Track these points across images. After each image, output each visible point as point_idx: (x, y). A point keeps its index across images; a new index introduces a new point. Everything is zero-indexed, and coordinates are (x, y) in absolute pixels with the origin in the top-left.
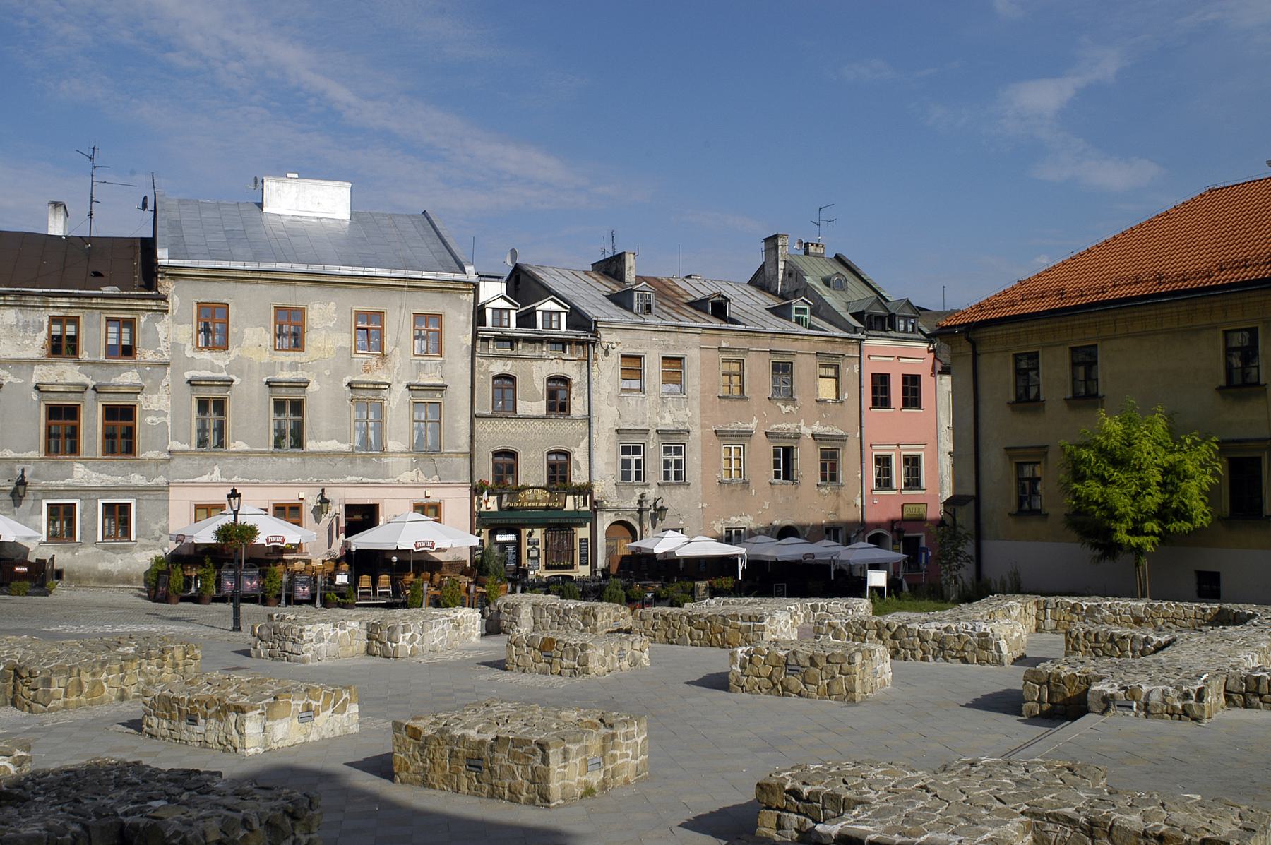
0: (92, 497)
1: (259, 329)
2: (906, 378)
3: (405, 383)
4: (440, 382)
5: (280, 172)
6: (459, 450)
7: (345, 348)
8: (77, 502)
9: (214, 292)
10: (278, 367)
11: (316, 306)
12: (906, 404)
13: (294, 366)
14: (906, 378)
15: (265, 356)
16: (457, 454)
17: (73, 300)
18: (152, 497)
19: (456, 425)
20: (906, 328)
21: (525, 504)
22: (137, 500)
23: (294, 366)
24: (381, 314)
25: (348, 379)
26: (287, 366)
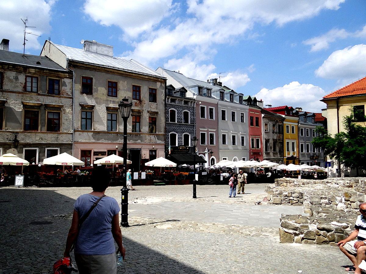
0: (43, 147)
1: (103, 88)
2: (256, 118)
3: (147, 110)
4: (156, 111)
8: (37, 149)
9: (88, 74)
14: (256, 118)
15: (105, 97)
17: (37, 70)
18: (66, 147)
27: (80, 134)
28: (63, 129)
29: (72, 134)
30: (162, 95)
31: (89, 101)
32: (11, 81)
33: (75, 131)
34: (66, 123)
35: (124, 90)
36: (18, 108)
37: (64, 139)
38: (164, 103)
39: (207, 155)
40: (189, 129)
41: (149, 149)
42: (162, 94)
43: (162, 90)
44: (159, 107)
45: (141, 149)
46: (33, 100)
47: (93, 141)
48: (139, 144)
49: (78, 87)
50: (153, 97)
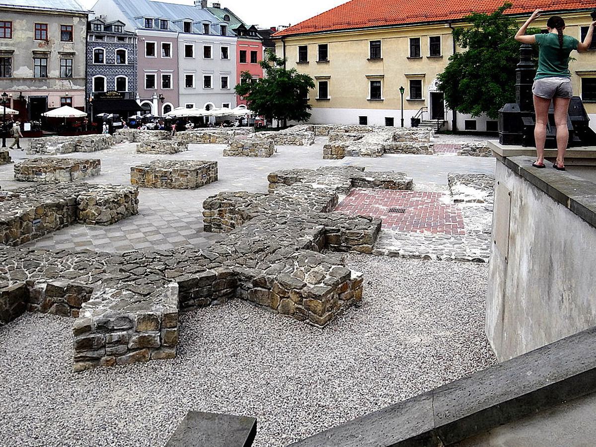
3: (57, 51)
4: (72, 51)
6: (81, 77)
7: (30, 38)
11: (17, 21)
12: (252, 61)
16: (79, 79)
20: (252, 33)
24: (46, 25)
30: (82, 32)
39: (155, 101)
41: (59, 96)
44: (78, 46)
48: (45, 91)
50: (67, 34)
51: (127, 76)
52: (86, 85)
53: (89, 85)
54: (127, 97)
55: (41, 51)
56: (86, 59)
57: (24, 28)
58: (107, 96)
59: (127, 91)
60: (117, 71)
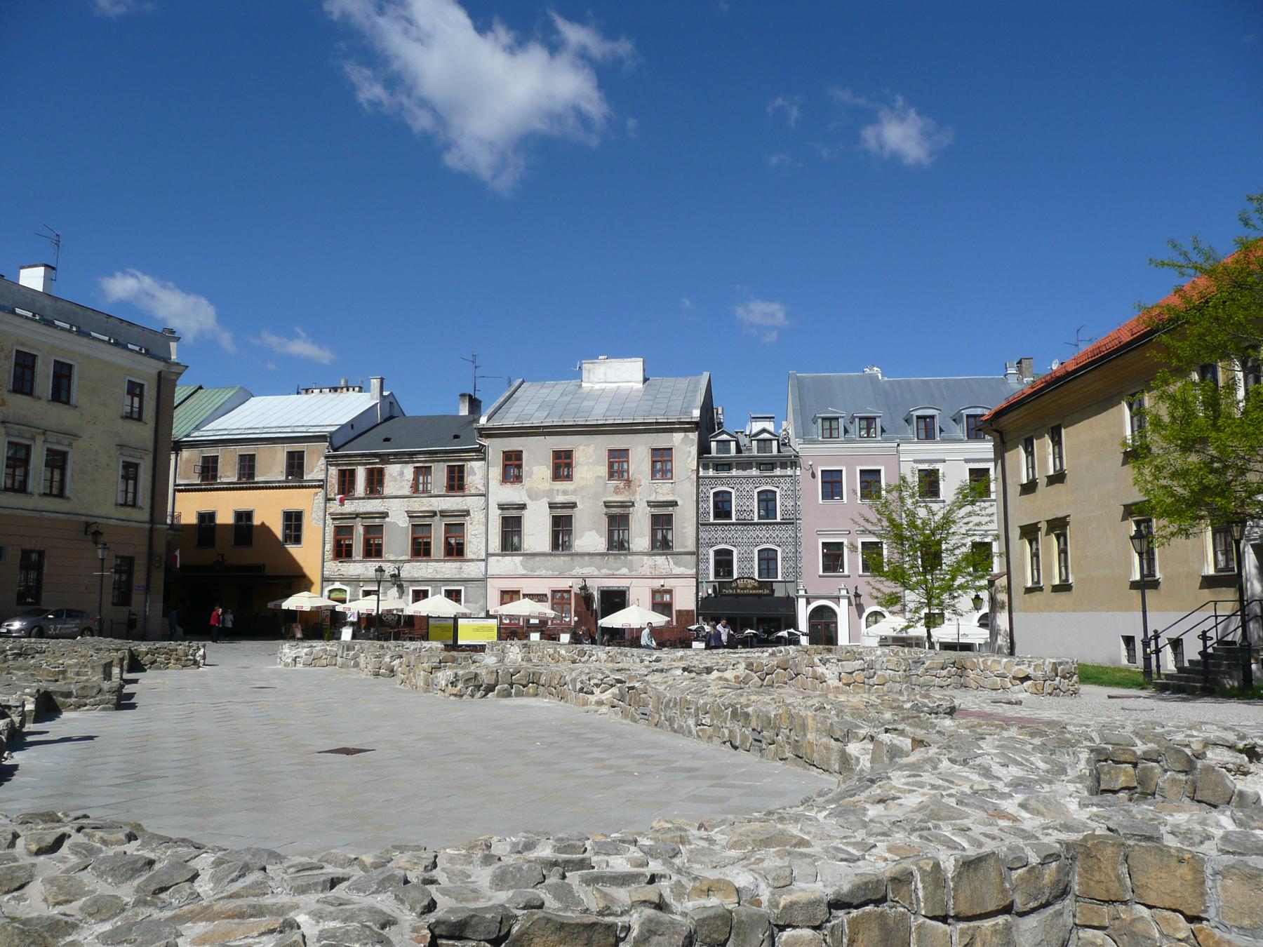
5: (593, 356)
7: (601, 477)
9: (513, 444)
10: (555, 493)
13: (565, 492)
19: (685, 531)
21: (738, 591)
22: (466, 587)
23: (565, 492)
25: (605, 499)
26: (563, 492)
27: (498, 561)
28: (469, 552)
29: (484, 560)
31: (511, 494)
32: (395, 479)
33: (488, 555)
34: (474, 540)
35: (588, 464)
36: (404, 522)
37: (471, 570)
38: (694, 477)
40: (777, 536)
42: (689, 456)
43: (688, 449)
45: (629, 588)
46: (423, 504)
47: (524, 572)
49: (496, 472)
51: (779, 546)
52: (698, 565)
53: (702, 566)
54: (779, 592)
55: (617, 502)
56: (697, 513)
57: (591, 461)
58: (737, 587)
59: (780, 578)
60: (758, 536)
